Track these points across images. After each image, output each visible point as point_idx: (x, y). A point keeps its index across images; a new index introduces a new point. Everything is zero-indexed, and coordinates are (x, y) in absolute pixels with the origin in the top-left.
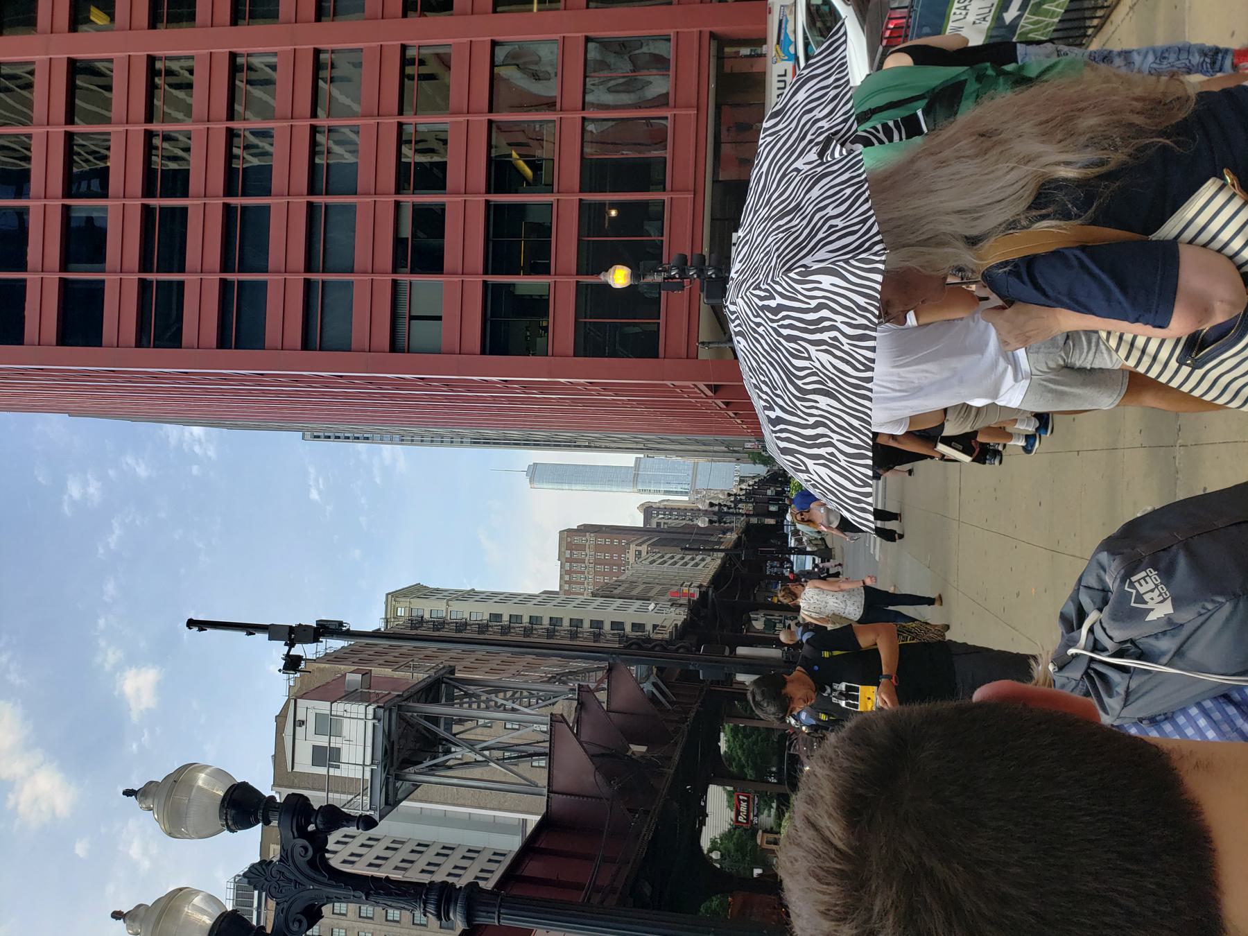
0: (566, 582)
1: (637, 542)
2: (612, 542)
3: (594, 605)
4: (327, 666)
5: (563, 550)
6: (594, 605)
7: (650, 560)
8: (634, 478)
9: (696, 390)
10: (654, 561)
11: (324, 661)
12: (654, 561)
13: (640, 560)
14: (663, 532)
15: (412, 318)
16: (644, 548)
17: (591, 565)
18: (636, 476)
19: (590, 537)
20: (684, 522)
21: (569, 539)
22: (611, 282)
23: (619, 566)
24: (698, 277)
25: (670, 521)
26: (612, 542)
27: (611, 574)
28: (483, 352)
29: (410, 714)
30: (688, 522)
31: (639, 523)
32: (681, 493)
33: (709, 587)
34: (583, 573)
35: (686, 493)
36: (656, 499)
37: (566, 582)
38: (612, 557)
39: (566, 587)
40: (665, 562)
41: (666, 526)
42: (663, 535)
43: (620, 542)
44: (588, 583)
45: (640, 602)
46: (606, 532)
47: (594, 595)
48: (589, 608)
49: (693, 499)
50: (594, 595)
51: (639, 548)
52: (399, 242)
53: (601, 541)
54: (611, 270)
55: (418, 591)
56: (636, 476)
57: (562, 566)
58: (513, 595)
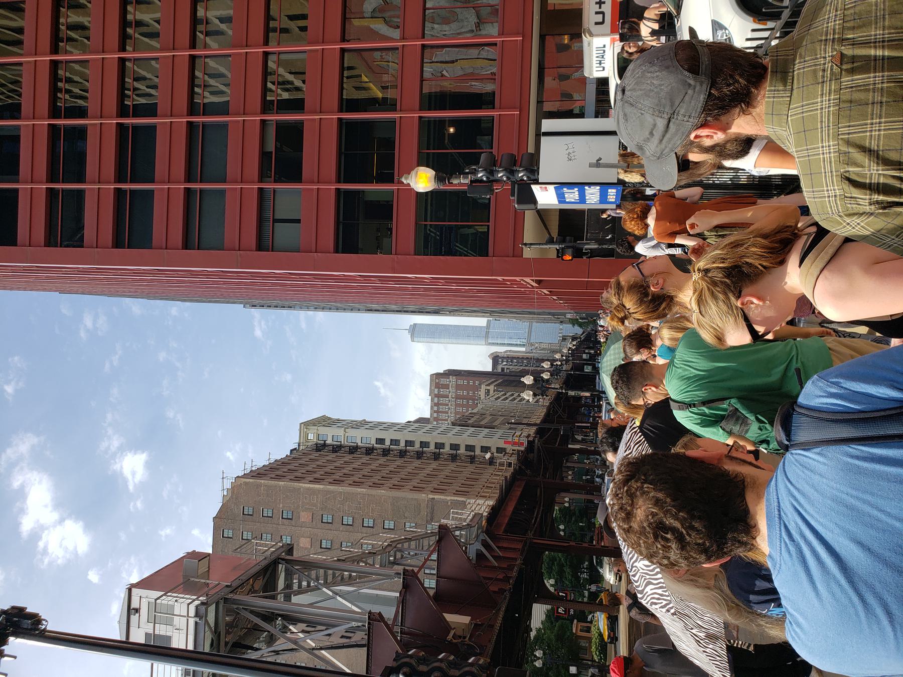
0: (435, 412)
1: (487, 383)
2: (468, 383)
3: (453, 432)
4: (251, 480)
6: (453, 432)
7: (495, 397)
8: (485, 335)
9: (522, 282)
10: (499, 398)
11: (249, 477)
12: (499, 398)
13: (489, 397)
14: (507, 375)
15: (275, 221)
16: (491, 388)
17: (453, 400)
18: (487, 333)
19: (453, 379)
20: (522, 368)
21: (437, 381)
22: (413, 185)
23: (474, 400)
24: (508, 178)
25: (511, 367)
26: (468, 383)
27: (467, 406)
28: (336, 251)
29: (235, 606)
30: (525, 368)
31: (488, 367)
32: (520, 345)
33: (535, 437)
34: (448, 405)
36: (501, 349)
37: (435, 412)
38: (468, 393)
39: (435, 415)
40: (507, 398)
41: (508, 371)
42: (506, 378)
43: (474, 383)
44: (451, 413)
45: (487, 430)
46: (463, 375)
47: (454, 424)
48: (450, 435)
49: (528, 350)
50: (454, 424)
51: (488, 388)
52: (264, 155)
53: (460, 382)
54: (413, 173)
55: (324, 421)
56: (487, 333)
57: (432, 400)
58: (394, 425)
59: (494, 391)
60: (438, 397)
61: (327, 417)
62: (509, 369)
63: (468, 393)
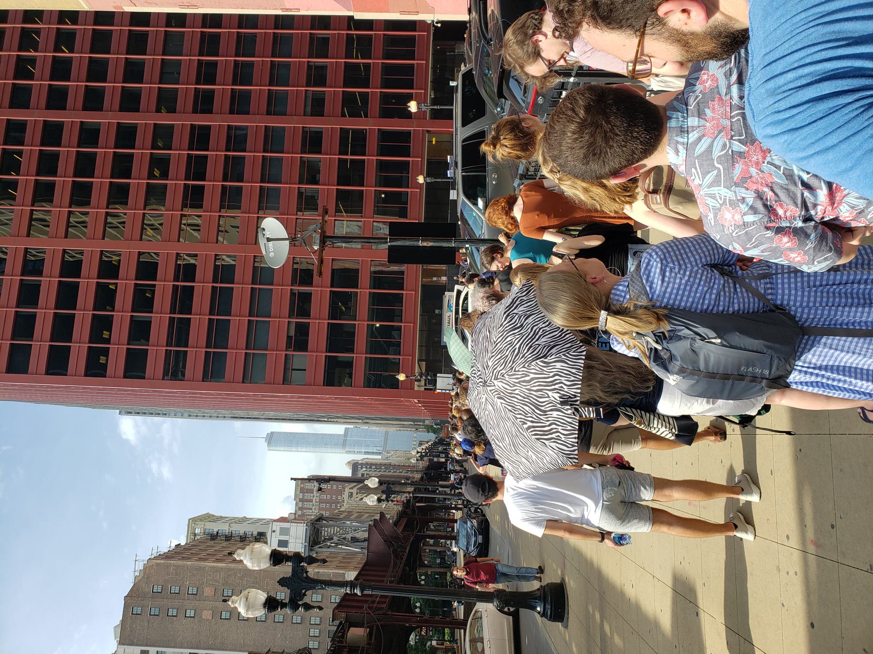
5: (298, 493)
13: (352, 499)
31: (347, 473)
32: (376, 453)
35: (380, 454)
36: (359, 458)
51: (351, 491)
55: (208, 518)
59: (357, 494)
60: (303, 502)
61: (211, 515)
62: (369, 474)
63: (332, 497)
